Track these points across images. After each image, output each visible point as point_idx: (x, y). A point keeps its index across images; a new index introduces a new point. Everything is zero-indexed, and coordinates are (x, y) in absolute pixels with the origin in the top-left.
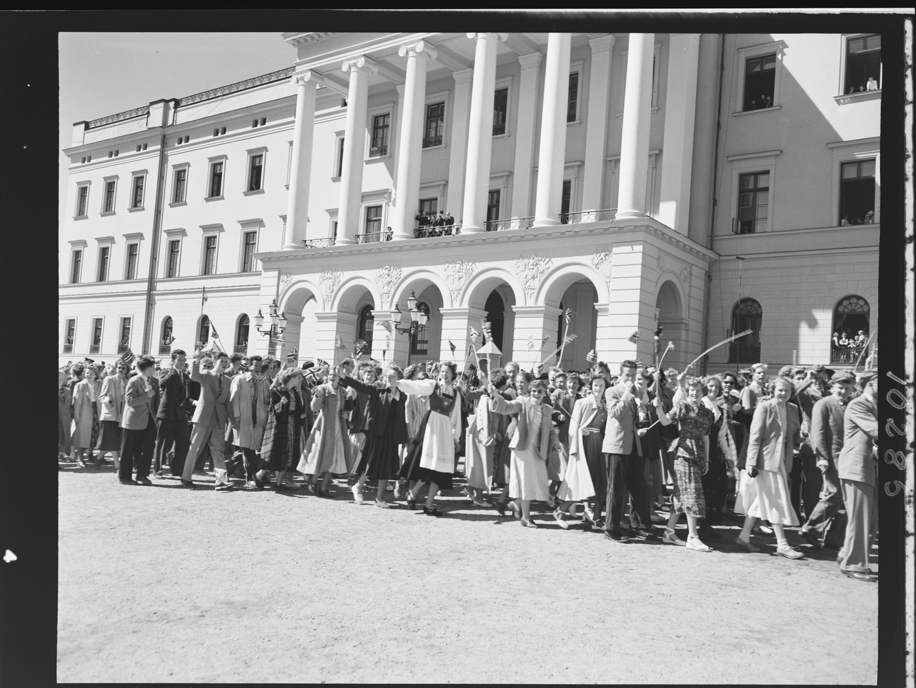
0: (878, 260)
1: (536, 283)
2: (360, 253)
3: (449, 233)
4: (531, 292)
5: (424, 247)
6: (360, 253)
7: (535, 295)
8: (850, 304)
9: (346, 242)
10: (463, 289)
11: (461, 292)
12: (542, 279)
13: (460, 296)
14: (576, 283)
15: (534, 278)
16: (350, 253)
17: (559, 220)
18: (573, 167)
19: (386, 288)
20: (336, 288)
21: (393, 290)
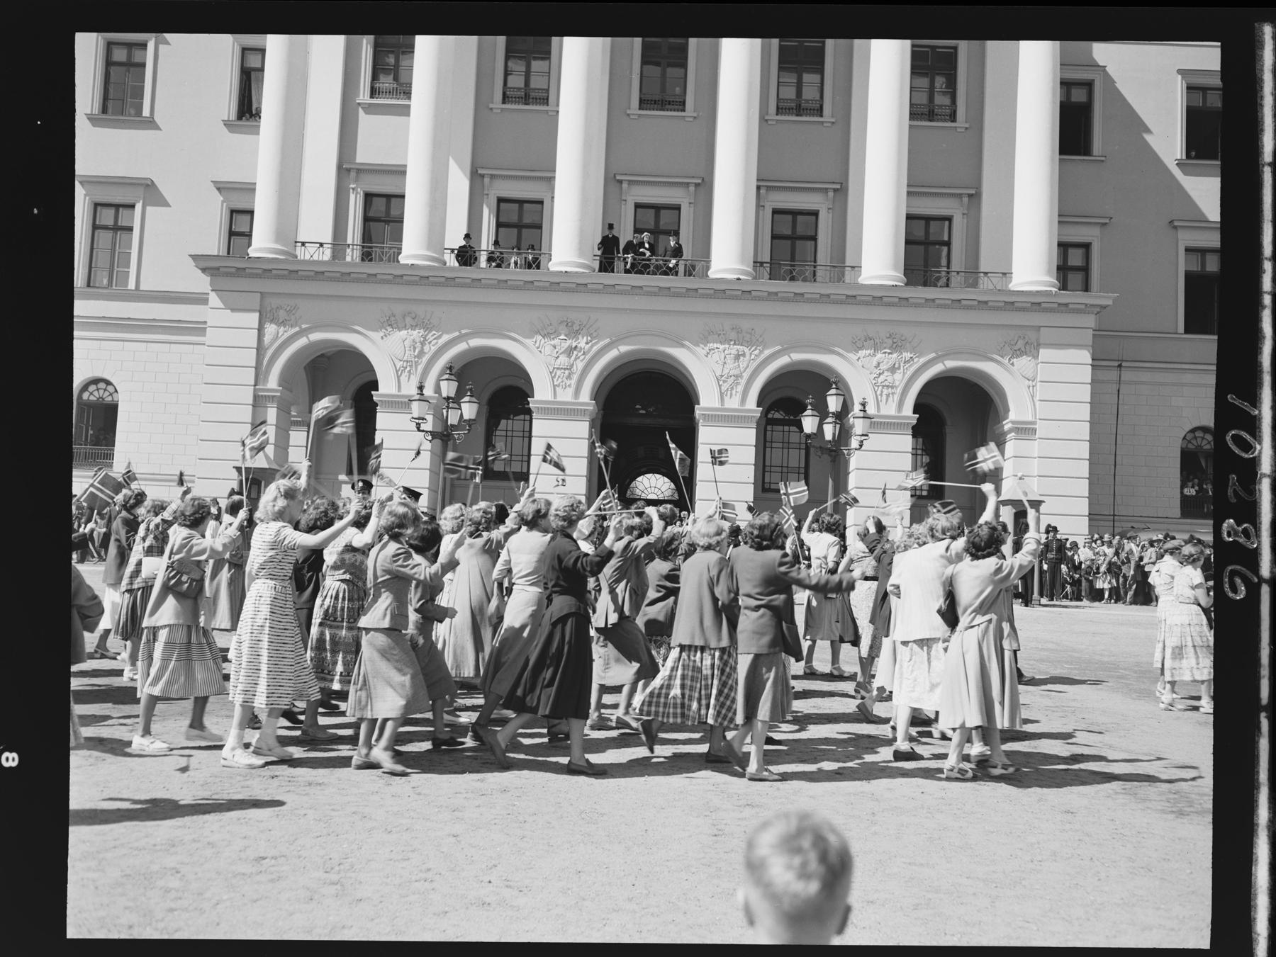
0: (1214, 382)
1: (899, 378)
2: (345, 277)
3: (689, 272)
4: (885, 391)
5: (772, 296)
6: (345, 277)
7: (896, 397)
8: (1196, 438)
9: (581, 266)
10: (746, 376)
11: (743, 381)
12: (909, 373)
13: (740, 388)
14: (322, 355)
15: (893, 369)
16: (581, 288)
17: (596, 265)
18: (960, 196)
19: (563, 360)
20: (430, 349)
21: (580, 365)
